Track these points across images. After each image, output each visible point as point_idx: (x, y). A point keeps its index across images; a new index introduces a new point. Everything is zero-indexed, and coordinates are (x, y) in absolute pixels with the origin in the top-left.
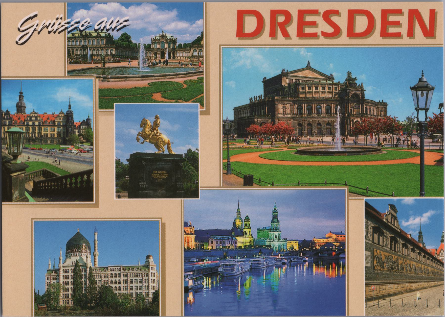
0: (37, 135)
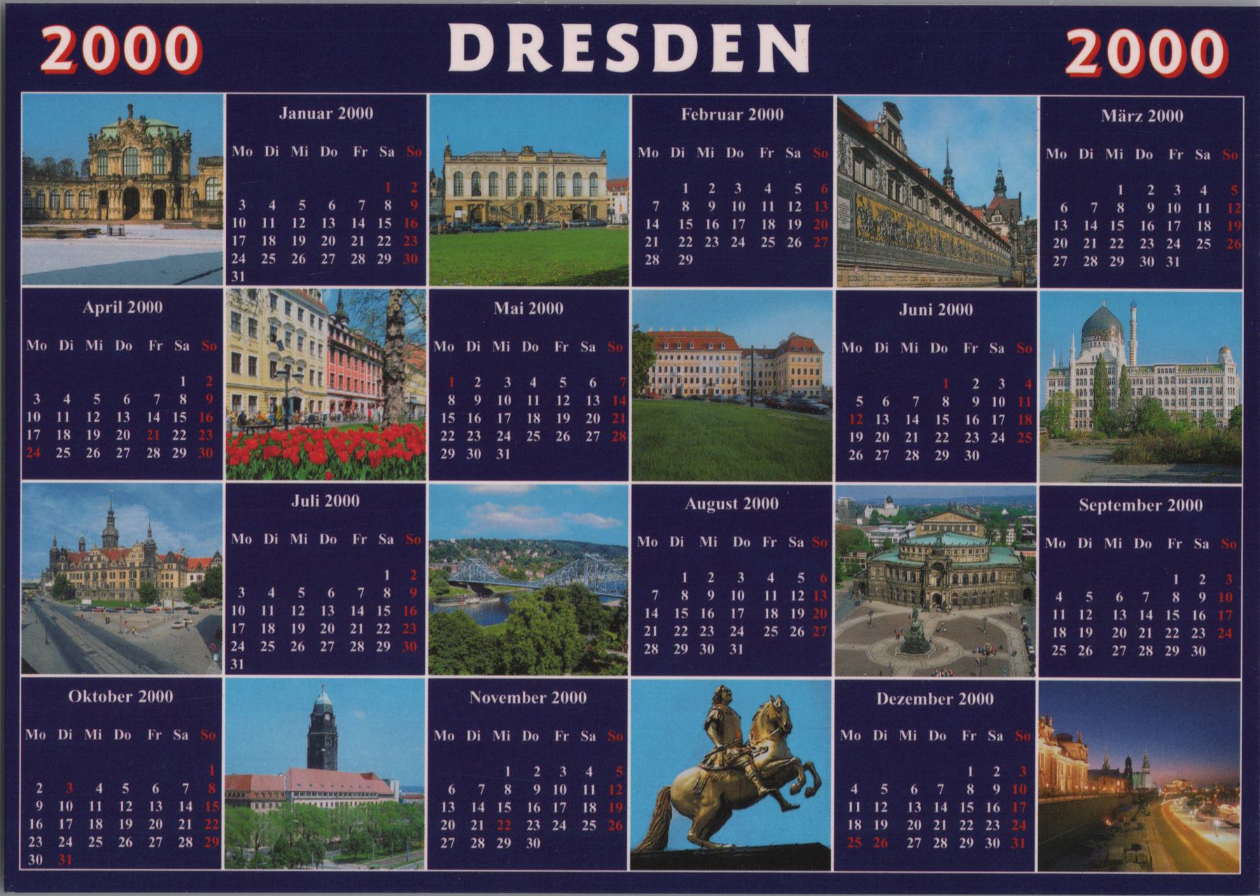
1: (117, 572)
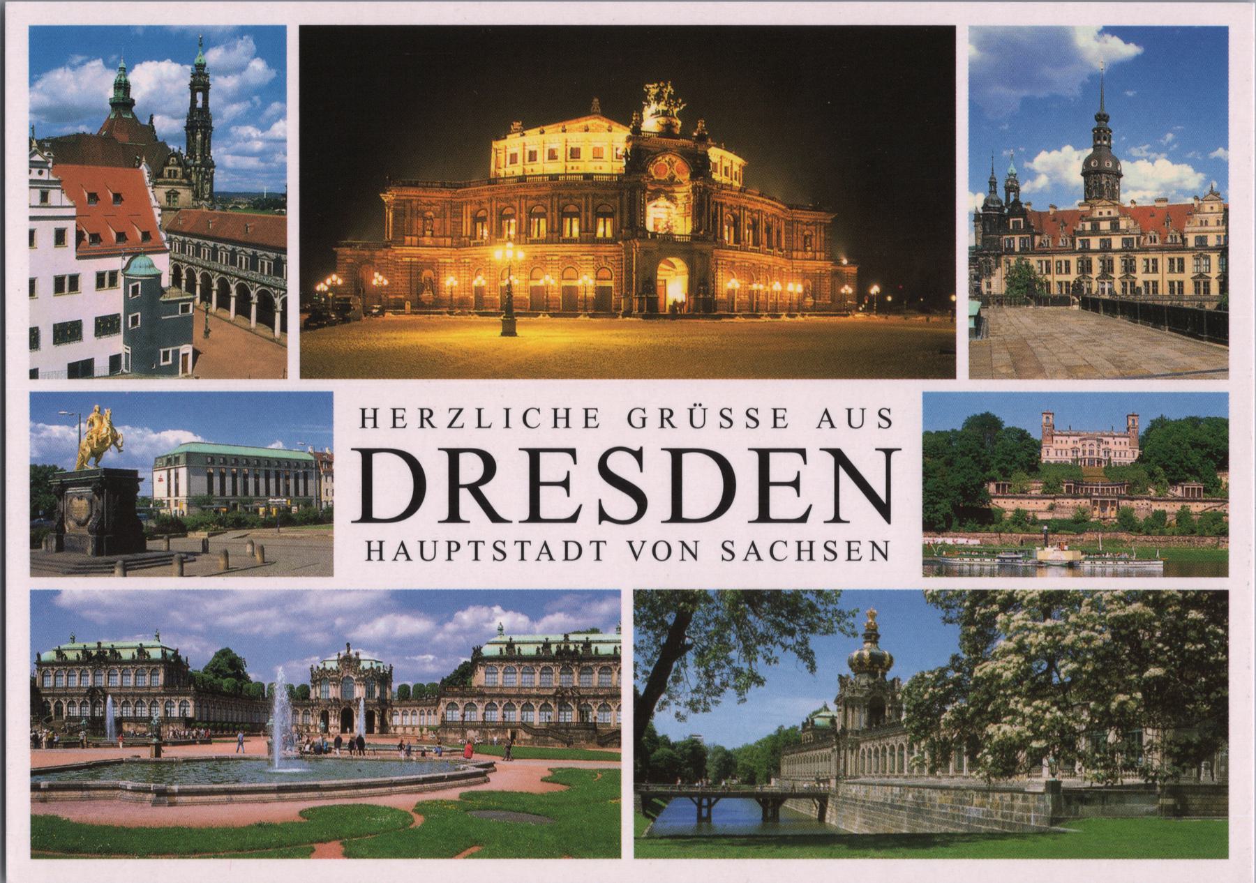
0: (1118, 287)
1: (1163, 260)
